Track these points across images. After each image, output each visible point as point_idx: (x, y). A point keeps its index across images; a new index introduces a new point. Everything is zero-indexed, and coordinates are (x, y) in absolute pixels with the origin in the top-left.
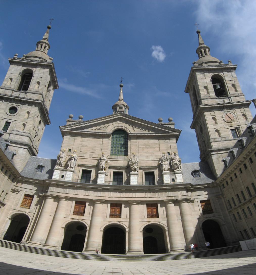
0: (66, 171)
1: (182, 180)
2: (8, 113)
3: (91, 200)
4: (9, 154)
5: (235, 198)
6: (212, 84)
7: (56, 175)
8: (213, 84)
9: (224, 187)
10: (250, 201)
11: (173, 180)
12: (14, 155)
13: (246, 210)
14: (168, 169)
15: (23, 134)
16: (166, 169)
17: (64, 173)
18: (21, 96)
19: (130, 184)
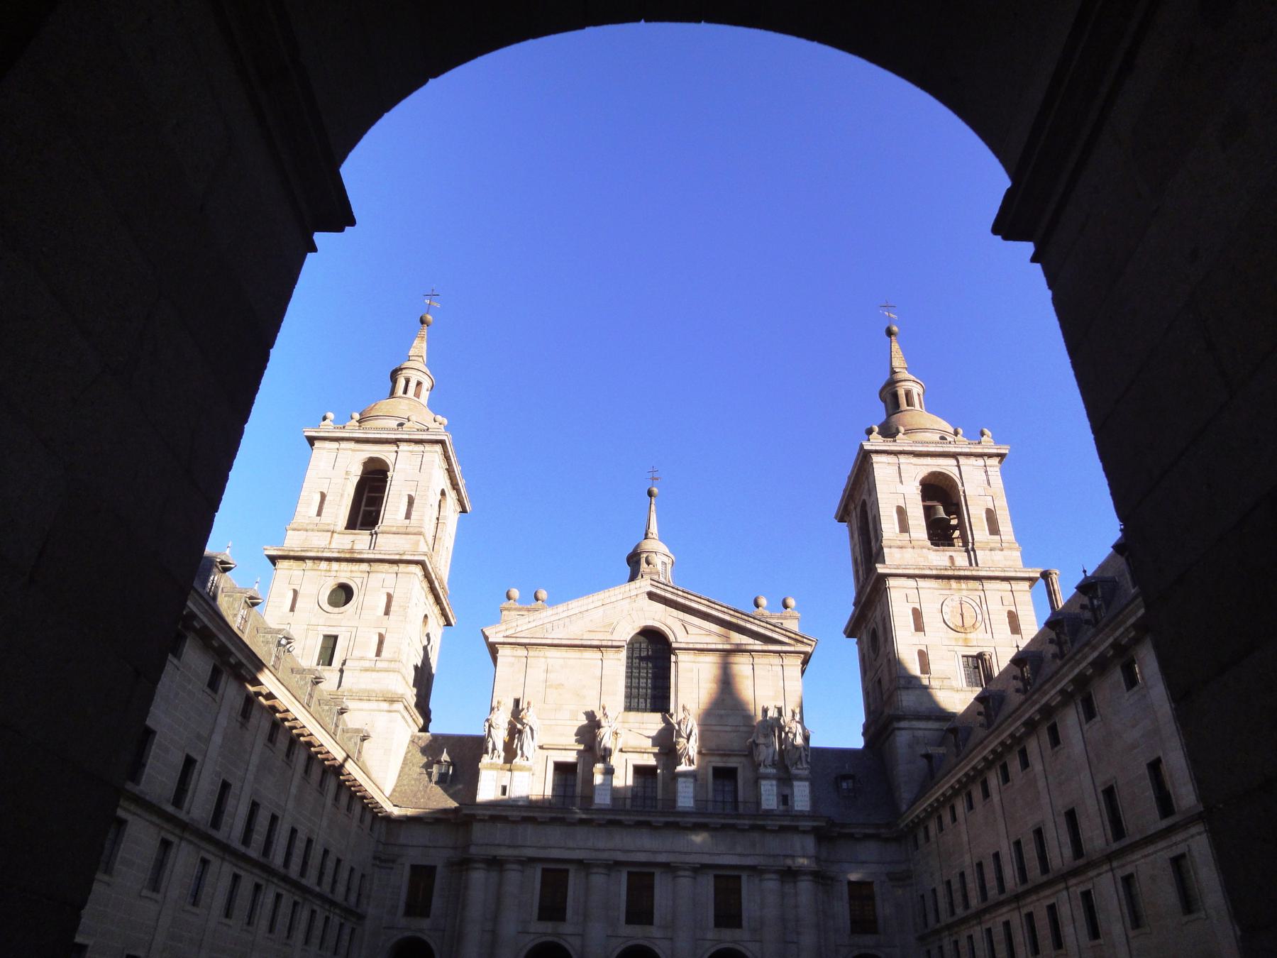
0: (510, 770)
1: (808, 804)
2: (326, 606)
3: (580, 862)
4: (350, 739)
5: (941, 891)
6: (921, 503)
7: (487, 791)
8: (923, 500)
9: (917, 846)
10: (979, 915)
11: (785, 799)
12: (364, 739)
13: (963, 942)
14: (773, 761)
15: (379, 665)
16: (769, 761)
17: (505, 778)
18: (357, 547)
19: (674, 807)
